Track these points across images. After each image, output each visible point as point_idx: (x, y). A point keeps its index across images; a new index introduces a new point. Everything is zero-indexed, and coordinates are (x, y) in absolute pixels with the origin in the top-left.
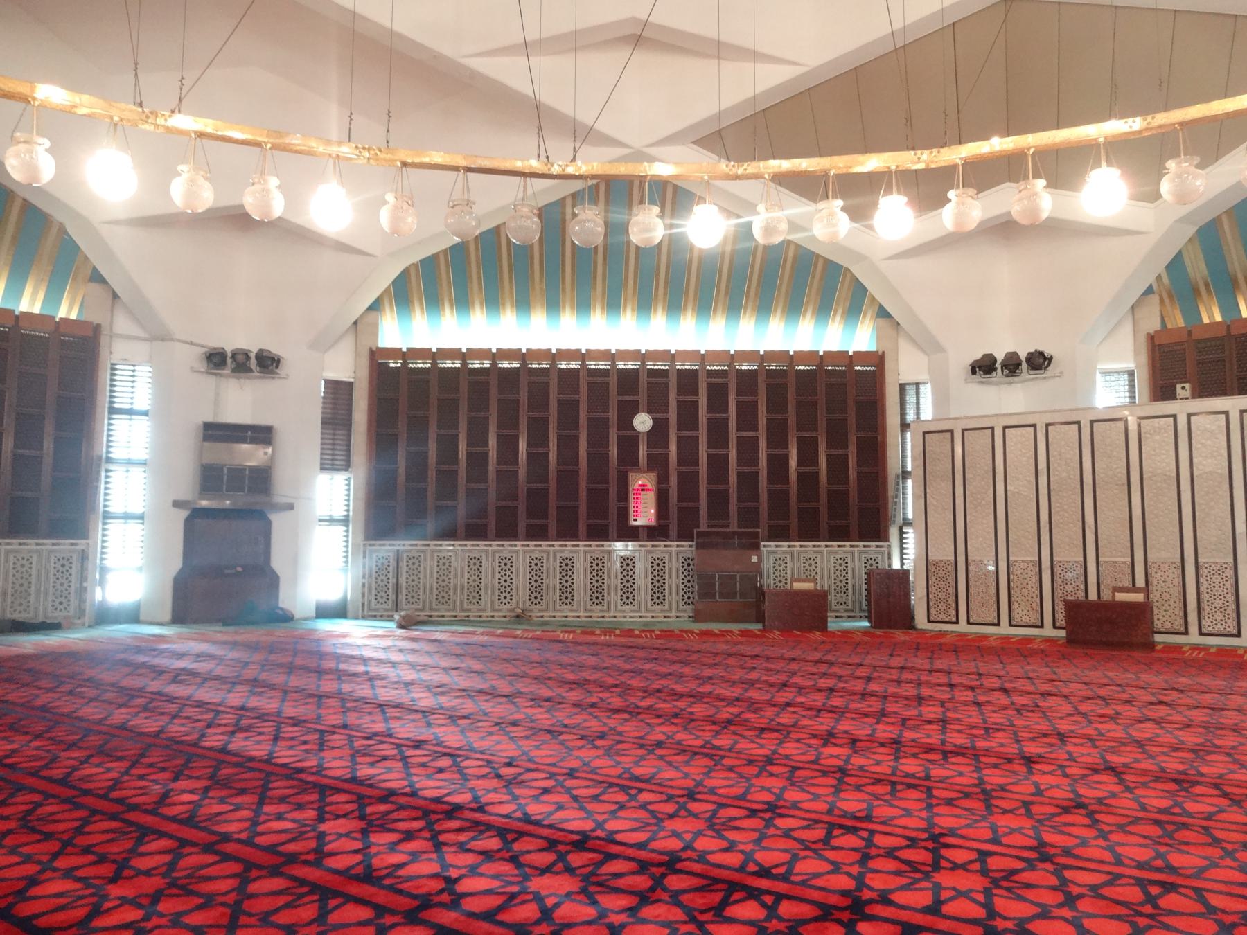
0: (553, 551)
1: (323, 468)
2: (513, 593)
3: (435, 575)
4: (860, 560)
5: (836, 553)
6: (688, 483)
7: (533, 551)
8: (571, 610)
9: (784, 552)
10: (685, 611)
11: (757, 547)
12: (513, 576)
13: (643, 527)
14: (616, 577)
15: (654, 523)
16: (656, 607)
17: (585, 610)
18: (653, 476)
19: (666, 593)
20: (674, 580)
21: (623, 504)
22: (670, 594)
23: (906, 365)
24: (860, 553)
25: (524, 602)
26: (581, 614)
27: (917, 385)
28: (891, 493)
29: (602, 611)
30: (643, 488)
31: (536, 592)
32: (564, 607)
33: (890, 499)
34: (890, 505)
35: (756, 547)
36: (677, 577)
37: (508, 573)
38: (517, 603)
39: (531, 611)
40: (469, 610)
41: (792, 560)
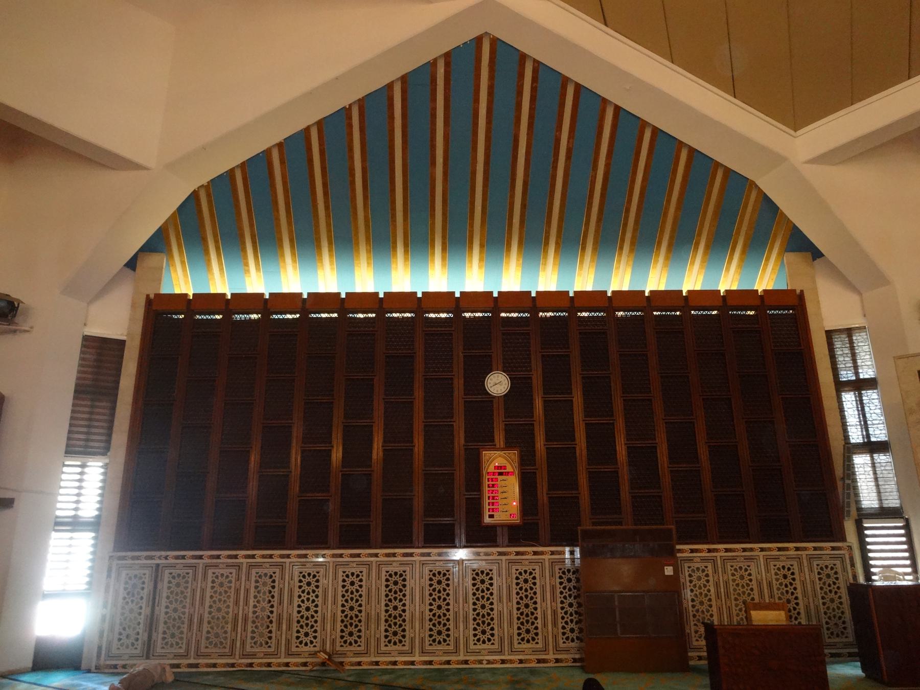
0: (376, 562)
1: (70, 451)
2: (318, 627)
3: (208, 602)
4: (811, 570)
5: (776, 558)
6: (562, 461)
7: (347, 564)
8: (401, 653)
9: (704, 560)
10: (567, 651)
11: (672, 552)
12: (319, 601)
13: (502, 526)
14: (466, 601)
15: (517, 520)
16: (525, 645)
17: (423, 652)
18: (514, 454)
19: (539, 623)
20: (549, 604)
21: (473, 495)
22: (545, 625)
23: (831, 307)
24: (810, 558)
25: (333, 642)
26: (417, 658)
27: (849, 332)
28: (839, 471)
29: (446, 653)
30: (501, 471)
31: (351, 623)
32: (391, 647)
33: (840, 484)
34: (840, 490)
35: (671, 553)
36: (553, 599)
37: (312, 596)
38: (324, 642)
39: (344, 654)
40: (253, 655)
41: (715, 571)
